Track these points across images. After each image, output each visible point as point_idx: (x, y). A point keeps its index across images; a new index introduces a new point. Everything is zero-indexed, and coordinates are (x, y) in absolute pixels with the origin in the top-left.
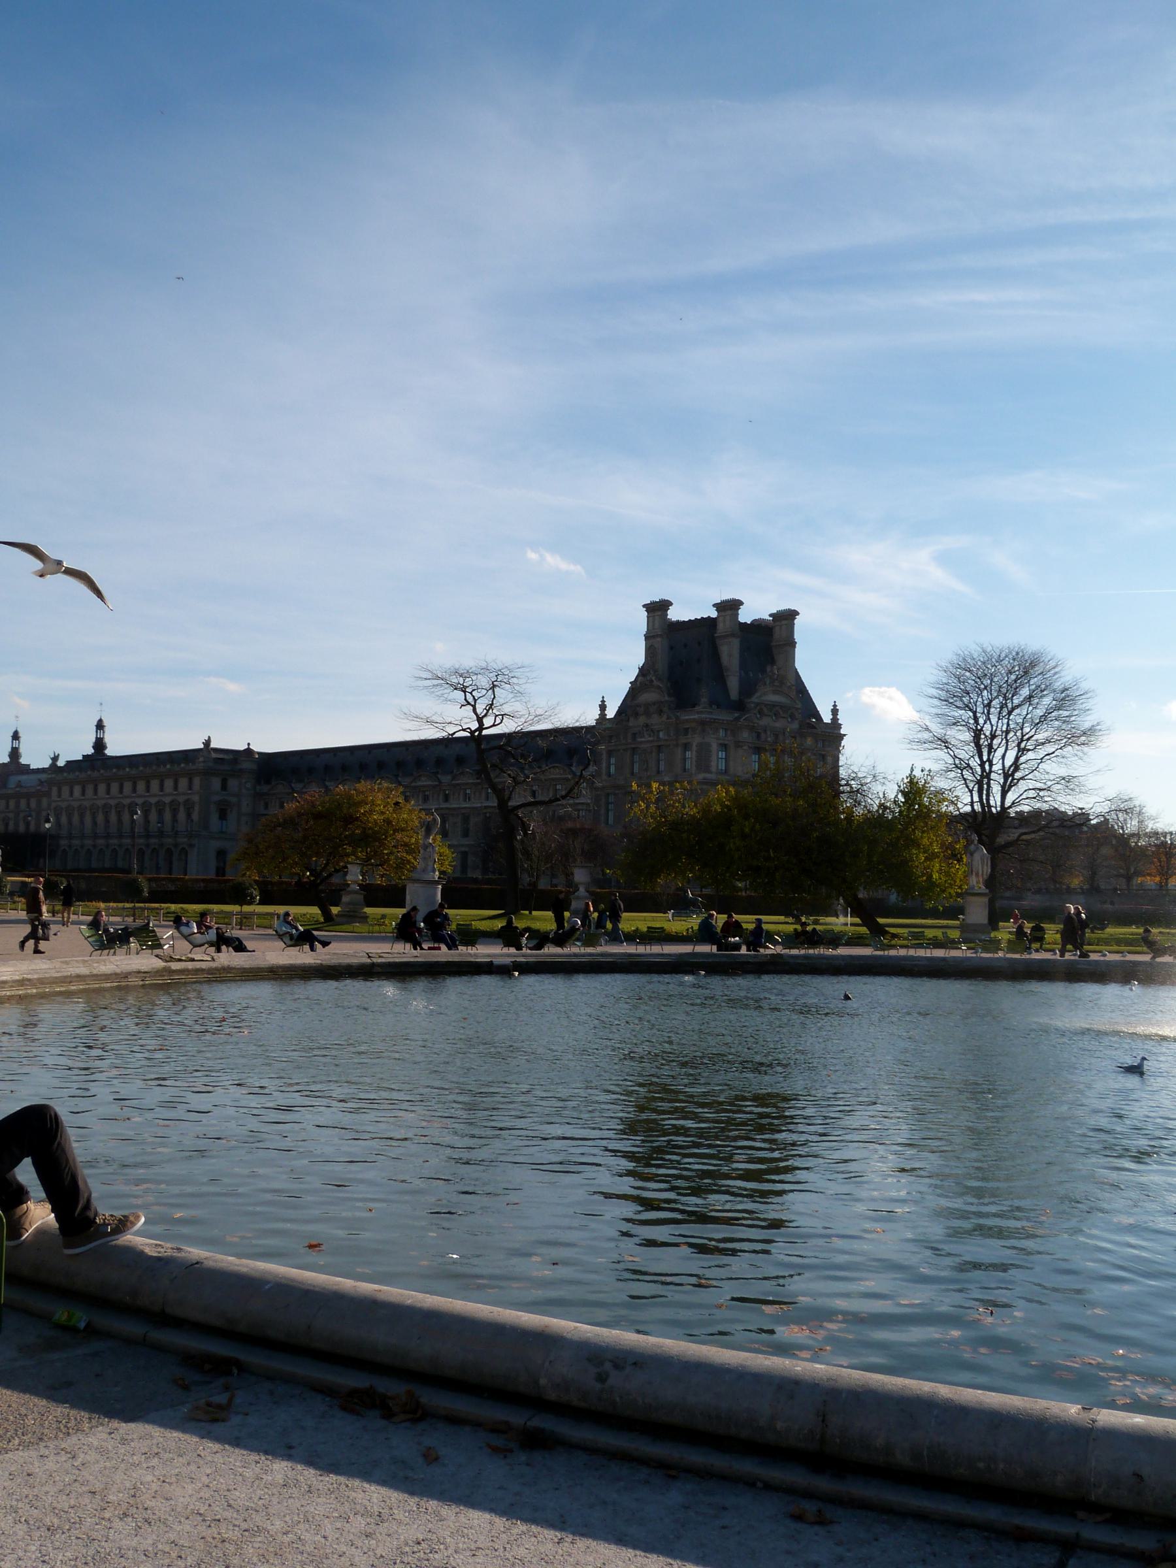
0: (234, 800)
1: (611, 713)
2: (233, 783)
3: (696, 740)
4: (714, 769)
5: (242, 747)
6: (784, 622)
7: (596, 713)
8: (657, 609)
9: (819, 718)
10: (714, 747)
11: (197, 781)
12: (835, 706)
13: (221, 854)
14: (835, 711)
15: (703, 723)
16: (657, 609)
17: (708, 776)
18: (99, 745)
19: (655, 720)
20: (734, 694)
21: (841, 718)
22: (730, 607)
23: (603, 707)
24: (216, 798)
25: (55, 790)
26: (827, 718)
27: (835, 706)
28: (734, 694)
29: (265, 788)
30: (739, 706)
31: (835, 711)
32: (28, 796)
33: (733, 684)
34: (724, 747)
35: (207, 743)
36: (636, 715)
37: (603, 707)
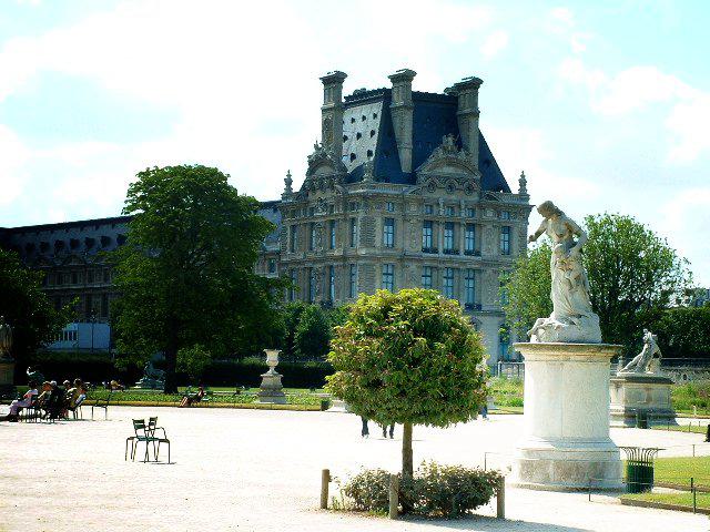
1: (297, 187)
3: (360, 214)
4: (378, 244)
6: (468, 91)
8: (333, 81)
9: (506, 189)
10: (379, 222)
12: (523, 176)
14: (523, 182)
15: (364, 197)
16: (333, 81)
17: (372, 251)
20: (406, 167)
21: (530, 189)
22: (404, 78)
23: (289, 182)
26: (515, 188)
27: (523, 176)
28: (406, 167)
30: (411, 179)
31: (523, 182)
33: (406, 155)
34: (390, 222)
36: (314, 190)
37: (289, 182)
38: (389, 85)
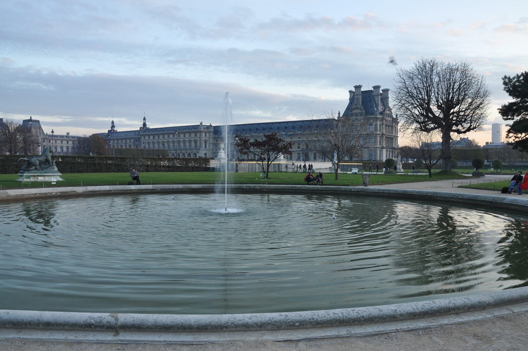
0: (208, 139)
2: (207, 134)
5: (209, 125)
7: (337, 115)
8: (358, 87)
11: (198, 135)
13: (205, 154)
18: (145, 125)
19: (359, 117)
22: (377, 88)
23: (339, 114)
24: (204, 139)
25: (142, 138)
29: (216, 136)
32: (122, 139)
35: (201, 123)
37: (339, 114)
38: (373, 89)
